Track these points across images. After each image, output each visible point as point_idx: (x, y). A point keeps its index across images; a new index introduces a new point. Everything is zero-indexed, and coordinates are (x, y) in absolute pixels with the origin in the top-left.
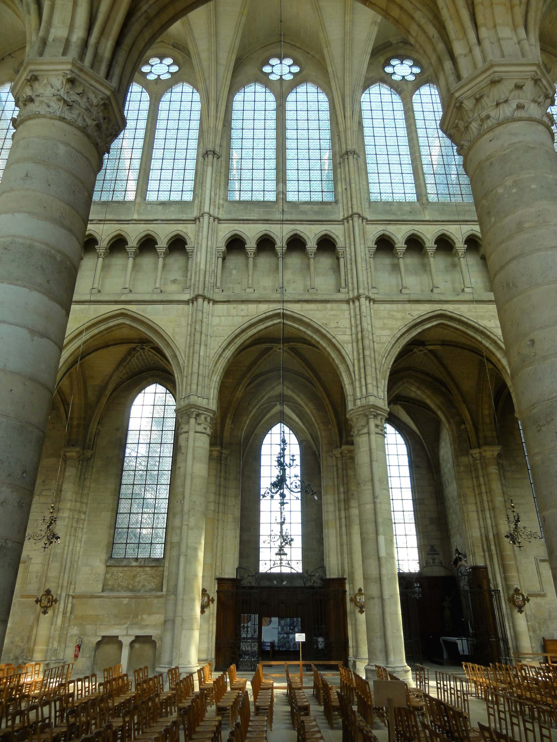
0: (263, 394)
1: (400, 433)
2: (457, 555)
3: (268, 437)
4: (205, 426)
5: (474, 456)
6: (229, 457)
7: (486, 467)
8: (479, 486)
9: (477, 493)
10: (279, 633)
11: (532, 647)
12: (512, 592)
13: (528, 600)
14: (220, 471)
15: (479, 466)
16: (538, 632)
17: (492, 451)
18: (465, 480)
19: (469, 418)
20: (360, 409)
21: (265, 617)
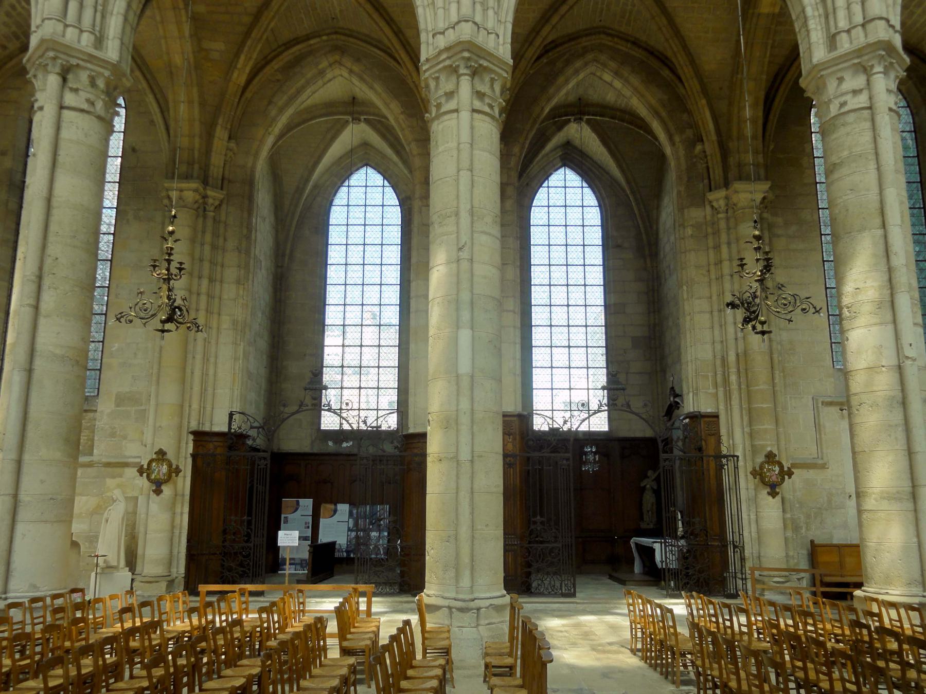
0: (299, 84)
1: (590, 186)
2: (672, 399)
3: (344, 190)
4: (92, 97)
5: (715, 204)
6: (224, 206)
7: (736, 225)
8: (719, 263)
9: (713, 277)
10: (349, 530)
11: (787, 556)
12: (760, 459)
13: (790, 474)
14: (204, 232)
15: (723, 224)
16: (803, 531)
17: (751, 192)
18: (693, 253)
19: (711, 126)
20: (444, 56)
21: (326, 502)
